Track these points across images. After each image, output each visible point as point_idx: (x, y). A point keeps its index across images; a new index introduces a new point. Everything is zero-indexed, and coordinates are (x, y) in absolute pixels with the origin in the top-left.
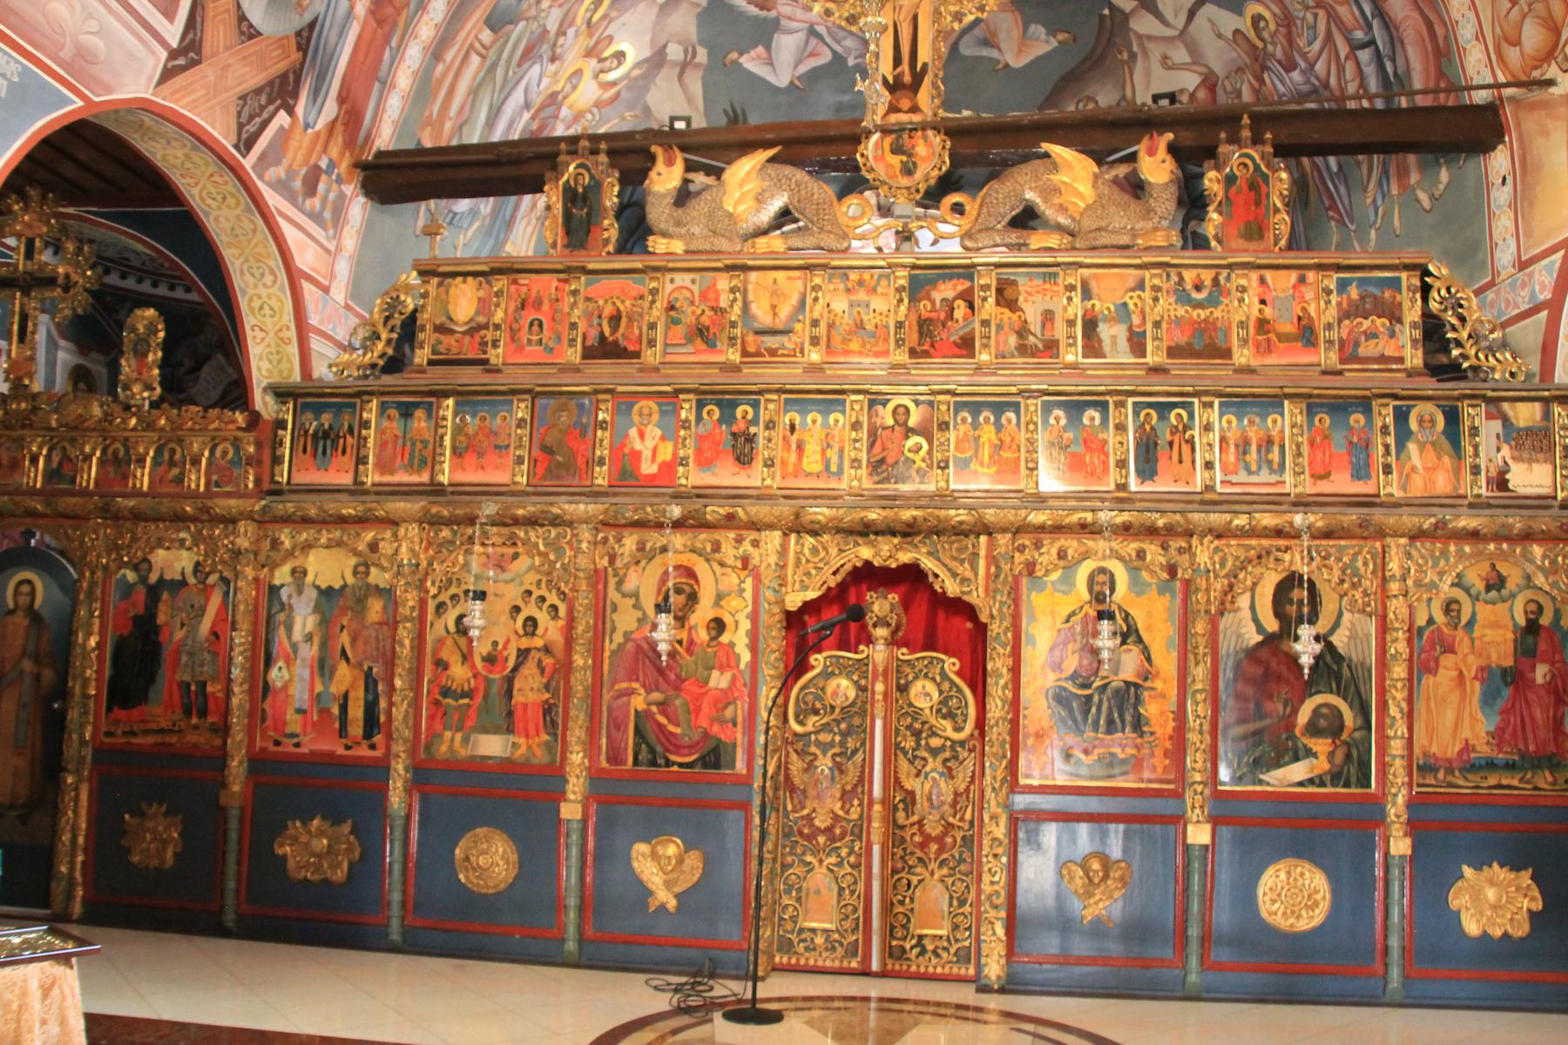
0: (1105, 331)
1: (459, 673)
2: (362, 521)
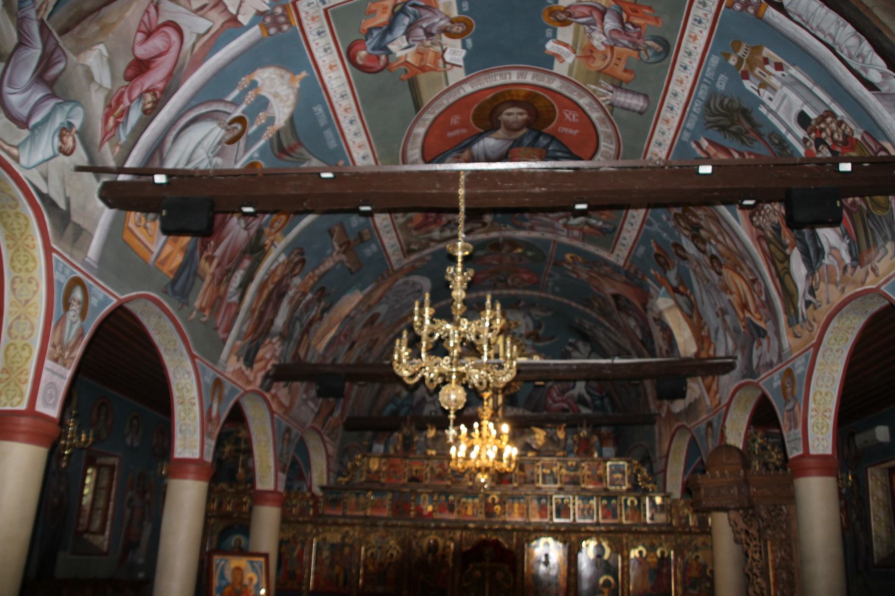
0: (548, 478)
1: (371, 568)
2: (345, 524)
